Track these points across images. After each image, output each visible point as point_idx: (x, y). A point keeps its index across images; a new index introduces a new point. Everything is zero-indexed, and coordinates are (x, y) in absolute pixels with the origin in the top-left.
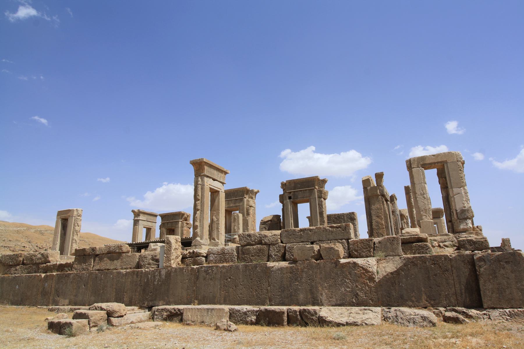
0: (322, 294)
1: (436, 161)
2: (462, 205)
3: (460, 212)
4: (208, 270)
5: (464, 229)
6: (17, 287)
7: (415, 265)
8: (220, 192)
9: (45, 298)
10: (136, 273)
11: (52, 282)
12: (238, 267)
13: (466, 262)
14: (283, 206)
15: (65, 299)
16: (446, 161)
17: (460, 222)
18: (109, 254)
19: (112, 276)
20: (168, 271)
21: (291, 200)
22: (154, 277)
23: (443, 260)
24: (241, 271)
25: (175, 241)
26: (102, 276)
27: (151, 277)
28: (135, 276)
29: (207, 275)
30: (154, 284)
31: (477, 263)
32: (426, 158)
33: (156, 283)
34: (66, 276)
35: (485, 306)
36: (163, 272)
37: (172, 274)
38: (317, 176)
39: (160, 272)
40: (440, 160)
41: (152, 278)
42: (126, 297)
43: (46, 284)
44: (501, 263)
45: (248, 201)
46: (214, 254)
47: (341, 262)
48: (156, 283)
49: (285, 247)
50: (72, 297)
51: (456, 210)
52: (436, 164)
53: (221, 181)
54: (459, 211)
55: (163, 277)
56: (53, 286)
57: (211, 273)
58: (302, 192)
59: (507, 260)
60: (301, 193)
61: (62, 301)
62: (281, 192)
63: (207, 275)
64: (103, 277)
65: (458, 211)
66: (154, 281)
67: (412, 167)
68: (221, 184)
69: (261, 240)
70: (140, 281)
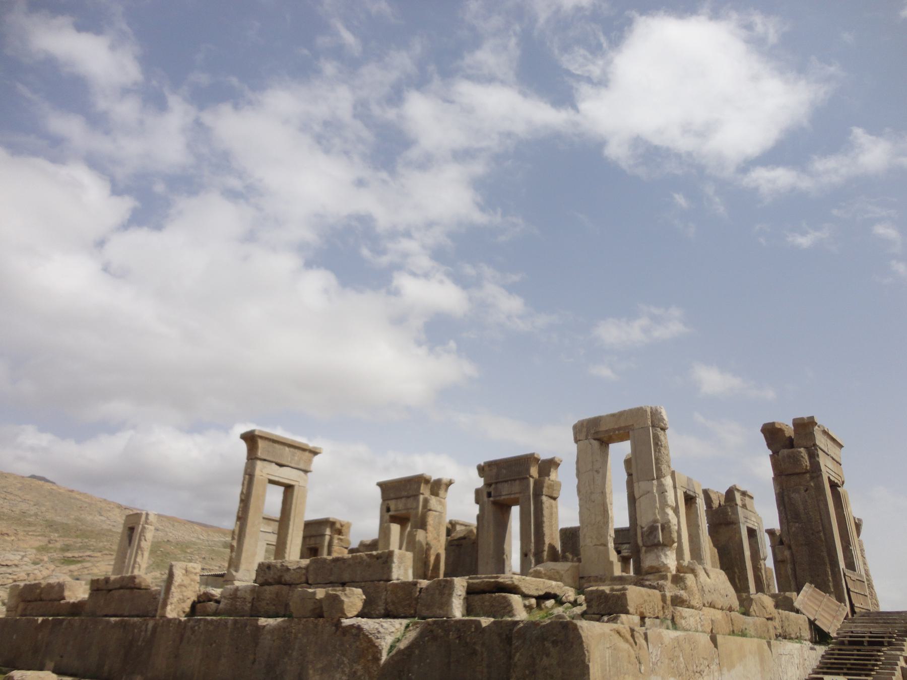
1: (616, 427)
2: (650, 518)
3: (647, 531)
4: (194, 627)
5: (652, 567)
7: (435, 638)
8: (296, 489)
12: (226, 623)
13: (504, 637)
14: (481, 510)
16: (633, 425)
17: (646, 552)
21: (491, 499)
23: (473, 630)
24: (229, 630)
25: (184, 572)
32: (600, 421)
38: (533, 454)
40: (623, 425)
44: (545, 643)
45: (426, 501)
47: (343, 625)
52: (617, 432)
53: (301, 466)
54: (645, 529)
55: (149, 633)
59: (555, 638)
60: (506, 485)
62: (480, 483)
65: (644, 528)
67: (578, 439)
68: (301, 473)
69: (281, 577)
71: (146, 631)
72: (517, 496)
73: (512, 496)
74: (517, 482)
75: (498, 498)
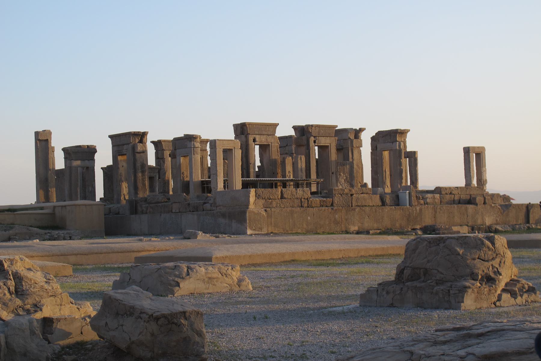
0: (486, 220)
6: (309, 218)
9: (338, 226)
10: (402, 208)
11: (342, 214)
15: (355, 226)
18: (362, 194)
19: (386, 210)
20: (421, 208)
22: (413, 211)
26: (380, 210)
27: (411, 211)
28: (402, 211)
29: (440, 210)
30: (413, 216)
31: (529, 208)
33: (414, 215)
34: (352, 210)
35: (531, 222)
36: (418, 208)
37: (423, 210)
39: (416, 208)
41: (412, 212)
42: (398, 224)
43: (337, 216)
46: (429, 198)
48: (414, 215)
49: (460, 197)
50: (360, 224)
51: (483, 180)
55: (418, 211)
56: (343, 217)
57: (442, 210)
58: (324, 138)
61: (352, 228)
63: (440, 210)
64: (381, 211)
66: (413, 214)
70: (405, 213)
71: (416, 210)
72: (328, 145)
73: (326, 145)
74: (329, 138)
75: (319, 145)
